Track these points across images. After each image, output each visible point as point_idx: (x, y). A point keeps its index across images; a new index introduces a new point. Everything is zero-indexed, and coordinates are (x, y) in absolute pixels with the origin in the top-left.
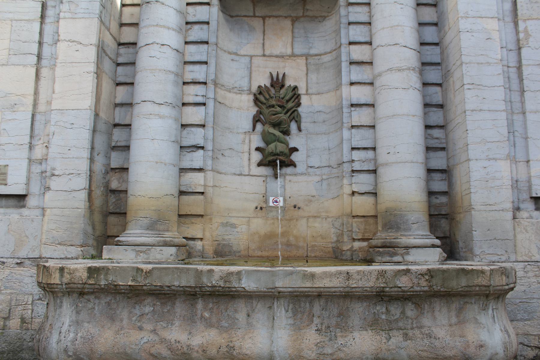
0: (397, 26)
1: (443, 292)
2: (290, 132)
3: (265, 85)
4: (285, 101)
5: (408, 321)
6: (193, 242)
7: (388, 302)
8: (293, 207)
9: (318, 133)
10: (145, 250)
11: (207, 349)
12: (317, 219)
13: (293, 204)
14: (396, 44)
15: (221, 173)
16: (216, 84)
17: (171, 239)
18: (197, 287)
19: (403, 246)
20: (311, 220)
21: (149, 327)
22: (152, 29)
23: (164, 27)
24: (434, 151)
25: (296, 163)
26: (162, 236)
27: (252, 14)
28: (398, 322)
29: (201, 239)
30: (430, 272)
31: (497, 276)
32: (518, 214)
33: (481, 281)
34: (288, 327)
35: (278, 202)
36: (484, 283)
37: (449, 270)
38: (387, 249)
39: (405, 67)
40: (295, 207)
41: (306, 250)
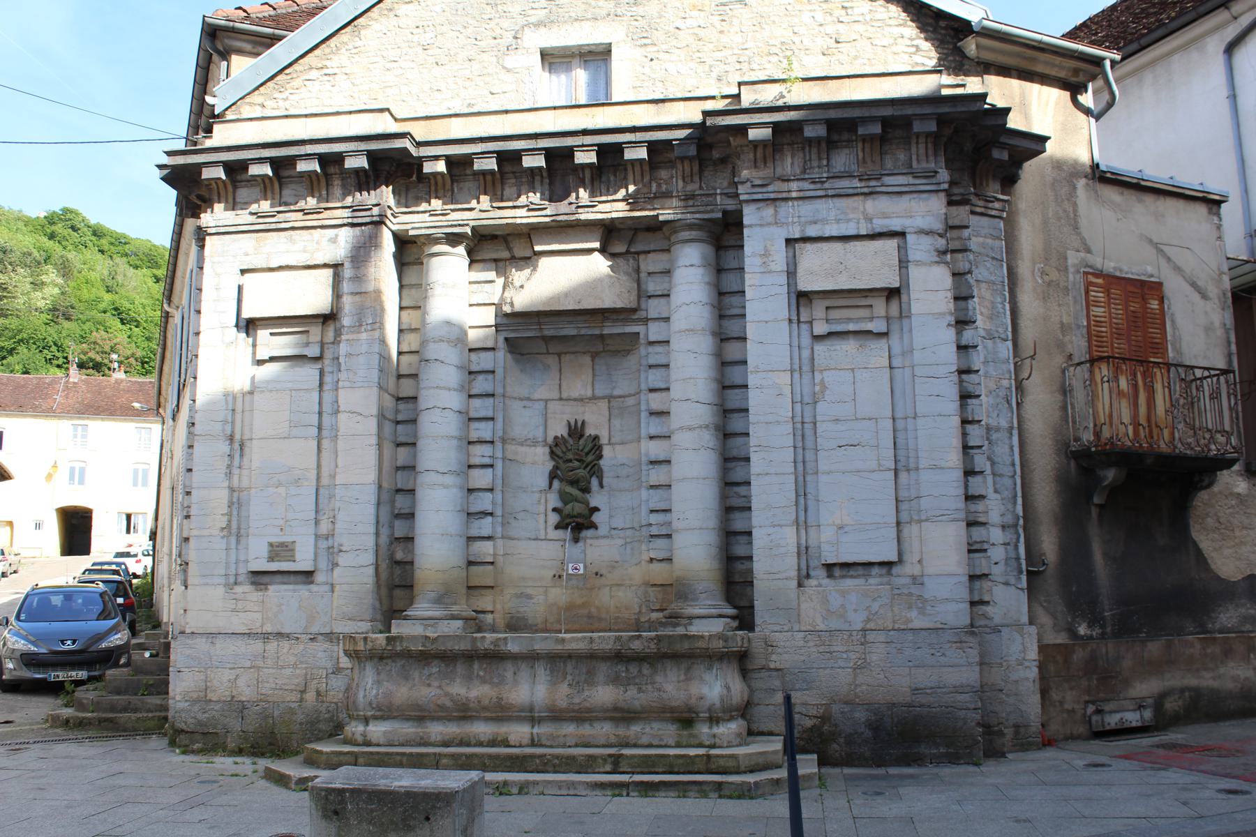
15: (513, 539)
16: (504, 441)
20: (614, 589)
21: (436, 684)
22: (432, 391)
23: (444, 388)
29: (492, 612)
32: (806, 582)
33: (702, 644)
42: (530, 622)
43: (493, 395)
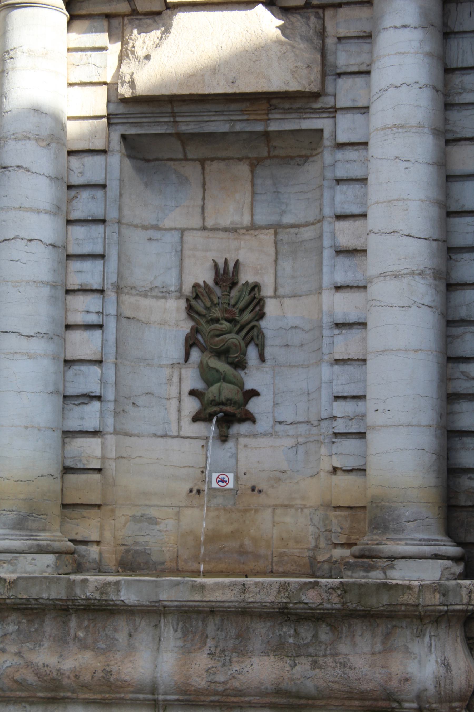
0: (398, 200)
1: (360, 611)
2: (246, 363)
3: (204, 282)
4: (237, 311)
5: (321, 646)
6: (84, 547)
7: (297, 623)
8: (250, 490)
10: (10, 559)
11: (80, 674)
12: (289, 510)
13: (249, 485)
14: (394, 232)
16: (119, 289)
17: (48, 542)
18: (69, 600)
19: (387, 556)
21: (13, 649)
23: (31, 210)
24: (470, 401)
25: (256, 416)
26: (35, 538)
27: (181, 156)
28: (308, 647)
29: (98, 543)
30: (343, 586)
31: (428, 593)
33: (408, 598)
34: (176, 650)
35: (226, 482)
36: (411, 602)
37: (368, 584)
38: (360, 560)
39: (405, 271)
40: (253, 489)
41: (270, 560)
42: (154, 558)
43: (103, 221)
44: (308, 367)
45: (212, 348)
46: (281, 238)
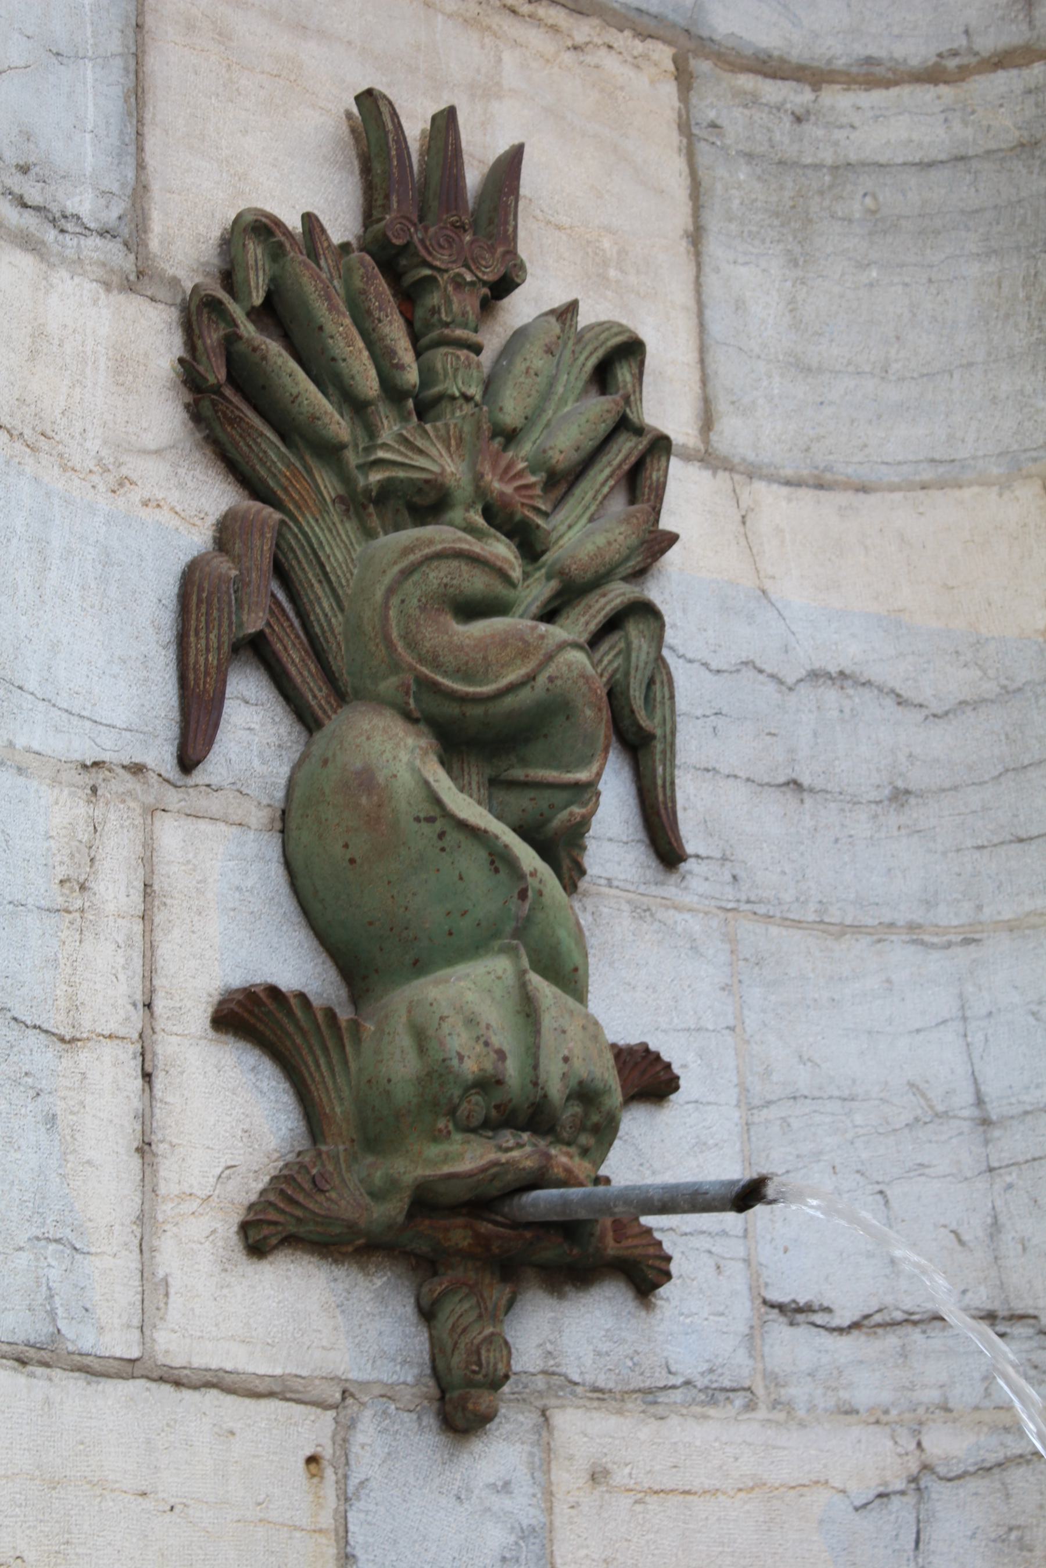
9: (834, 915)
44: (967, 942)
45: (435, 688)
46: (712, 114)
